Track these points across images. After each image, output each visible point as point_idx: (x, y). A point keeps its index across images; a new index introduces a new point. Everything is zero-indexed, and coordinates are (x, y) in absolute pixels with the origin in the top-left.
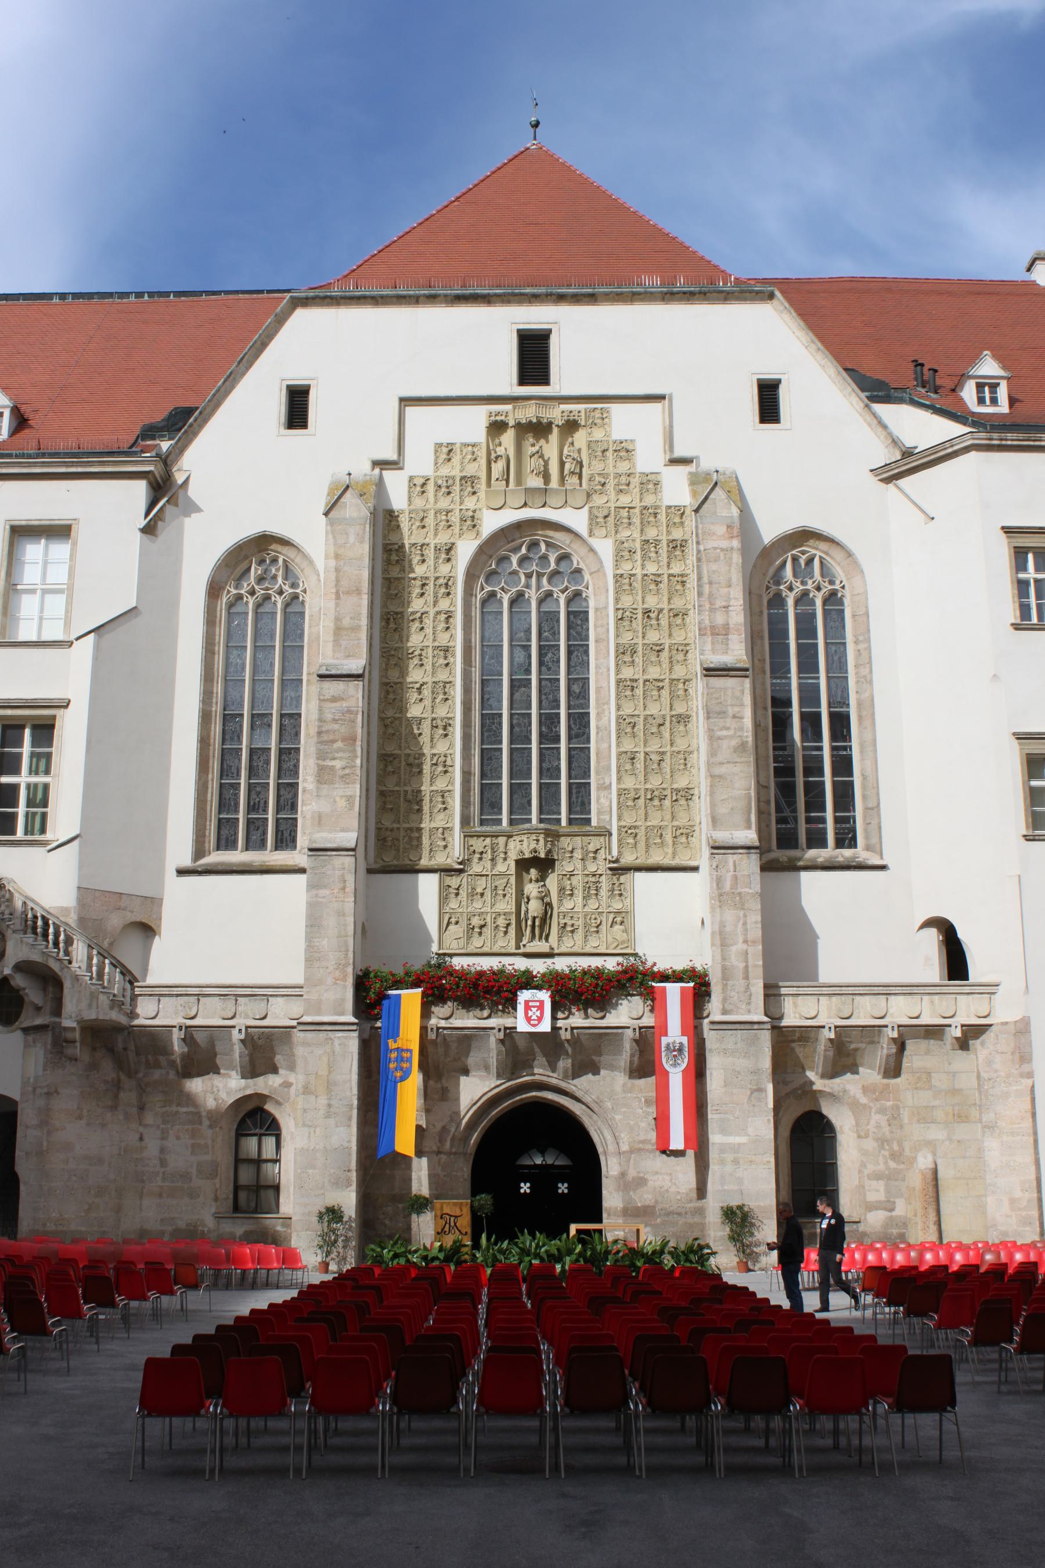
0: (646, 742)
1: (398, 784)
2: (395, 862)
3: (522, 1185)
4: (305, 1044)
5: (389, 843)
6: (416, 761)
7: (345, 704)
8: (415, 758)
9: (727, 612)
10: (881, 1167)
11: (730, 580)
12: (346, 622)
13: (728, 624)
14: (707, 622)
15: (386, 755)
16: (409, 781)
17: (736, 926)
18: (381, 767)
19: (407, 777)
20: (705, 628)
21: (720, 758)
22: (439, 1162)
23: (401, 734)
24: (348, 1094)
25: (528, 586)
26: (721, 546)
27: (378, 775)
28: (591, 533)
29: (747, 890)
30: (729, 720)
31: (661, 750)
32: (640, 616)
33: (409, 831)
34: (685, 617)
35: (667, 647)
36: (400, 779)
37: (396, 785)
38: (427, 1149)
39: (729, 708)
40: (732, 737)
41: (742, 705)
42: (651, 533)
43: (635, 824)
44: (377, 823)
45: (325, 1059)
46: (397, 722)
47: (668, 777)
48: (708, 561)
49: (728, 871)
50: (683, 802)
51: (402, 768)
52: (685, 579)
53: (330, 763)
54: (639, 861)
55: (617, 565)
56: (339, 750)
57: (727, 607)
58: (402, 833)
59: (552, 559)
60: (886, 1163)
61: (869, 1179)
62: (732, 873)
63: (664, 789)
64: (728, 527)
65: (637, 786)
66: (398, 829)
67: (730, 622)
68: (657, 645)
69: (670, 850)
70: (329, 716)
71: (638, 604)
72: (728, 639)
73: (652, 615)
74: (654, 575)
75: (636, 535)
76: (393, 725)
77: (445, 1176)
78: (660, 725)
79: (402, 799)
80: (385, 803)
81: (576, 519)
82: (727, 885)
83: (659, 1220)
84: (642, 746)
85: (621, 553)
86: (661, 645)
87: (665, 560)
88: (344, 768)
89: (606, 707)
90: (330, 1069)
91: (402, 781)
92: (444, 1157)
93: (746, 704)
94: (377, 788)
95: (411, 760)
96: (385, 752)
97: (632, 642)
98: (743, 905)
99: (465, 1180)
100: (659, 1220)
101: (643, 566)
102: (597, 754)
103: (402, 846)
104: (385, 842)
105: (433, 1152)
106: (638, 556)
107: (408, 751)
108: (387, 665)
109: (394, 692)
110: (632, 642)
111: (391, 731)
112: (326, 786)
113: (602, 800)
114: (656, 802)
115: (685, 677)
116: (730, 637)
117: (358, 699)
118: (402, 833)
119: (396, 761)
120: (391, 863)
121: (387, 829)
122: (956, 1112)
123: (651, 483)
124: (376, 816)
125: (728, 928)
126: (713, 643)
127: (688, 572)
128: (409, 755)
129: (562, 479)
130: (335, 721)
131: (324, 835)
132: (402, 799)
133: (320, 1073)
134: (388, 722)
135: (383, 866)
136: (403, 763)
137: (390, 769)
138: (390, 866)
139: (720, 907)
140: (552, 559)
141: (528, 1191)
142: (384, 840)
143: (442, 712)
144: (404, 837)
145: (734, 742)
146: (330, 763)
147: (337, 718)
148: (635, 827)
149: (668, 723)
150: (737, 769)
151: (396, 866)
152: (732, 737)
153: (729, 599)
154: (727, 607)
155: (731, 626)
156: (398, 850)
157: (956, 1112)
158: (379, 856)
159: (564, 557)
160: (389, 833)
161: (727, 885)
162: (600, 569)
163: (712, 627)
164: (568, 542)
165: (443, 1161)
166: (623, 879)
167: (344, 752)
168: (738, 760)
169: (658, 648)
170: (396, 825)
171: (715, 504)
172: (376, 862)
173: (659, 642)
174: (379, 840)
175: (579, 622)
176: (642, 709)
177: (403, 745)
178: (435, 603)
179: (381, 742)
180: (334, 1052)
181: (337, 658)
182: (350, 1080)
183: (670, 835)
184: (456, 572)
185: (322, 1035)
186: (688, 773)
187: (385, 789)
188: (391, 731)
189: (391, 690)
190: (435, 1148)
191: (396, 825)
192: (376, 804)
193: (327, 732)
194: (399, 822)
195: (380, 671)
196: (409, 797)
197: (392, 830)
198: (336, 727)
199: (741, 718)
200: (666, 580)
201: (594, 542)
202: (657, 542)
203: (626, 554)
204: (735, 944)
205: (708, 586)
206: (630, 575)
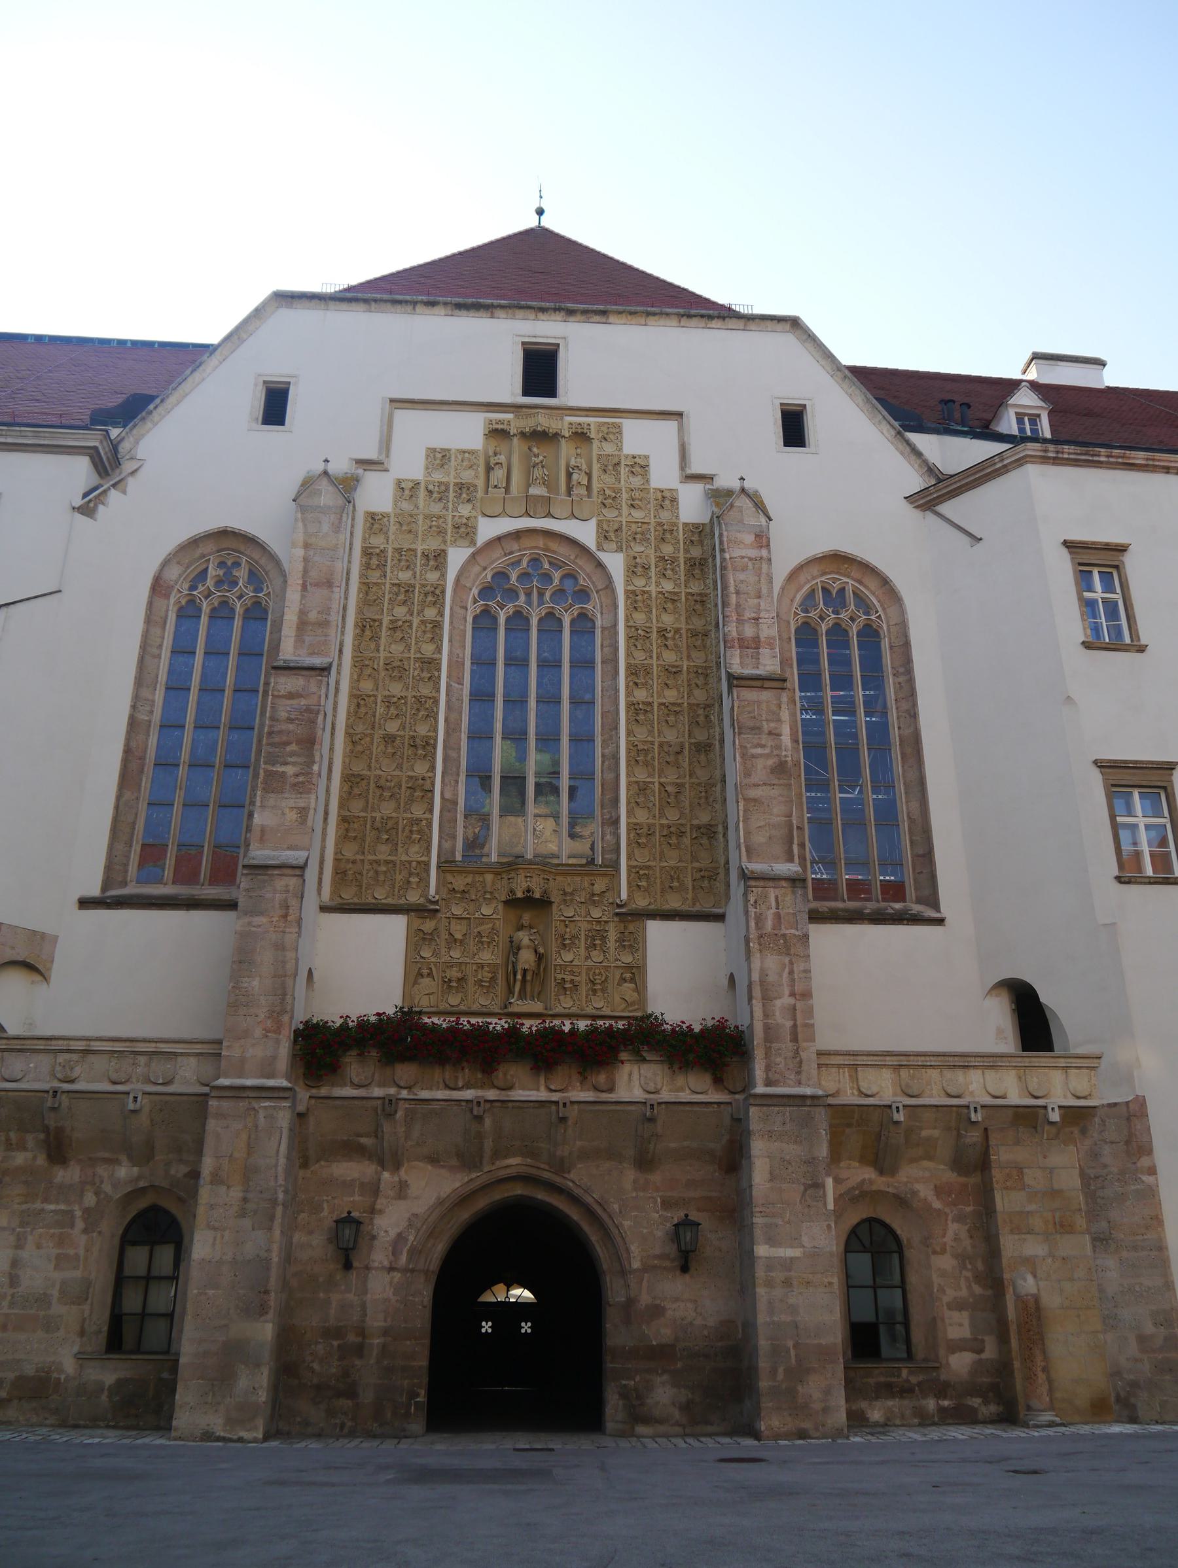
0: (661, 771)
1: (365, 809)
2: (356, 900)
3: (484, 1324)
4: (220, 1116)
5: (350, 877)
6: (388, 784)
7: (303, 702)
8: (387, 781)
9: (757, 625)
10: (964, 1293)
11: (759, 591)
12: (313, 616)
13: (758, 637)
14: (734, 634)
15: (353, 775)
16: (379, 806)
17: (781, 976)
18: (346, 788)
19: (376, 801)
20: (733, 641)
21: (755, 779)
22: (391, 1283)
23: (371, 753)
24: (272, 1183)
25: (529, 602)
26: (749, 555)
27: (341, 797)
28: (600, 548)
29: (793, 931)
30: (764, 736)
31: (678, 781)
32: (654, 635)
33: (375, 865)
34: (705, 638)
35: (685, 668)
36: (367, 803)
37: (362, 811)
38: (376, 1264)
39: (764, 723)
40: (767, 756)
41: (779, 720)
42: (667, 549)
43: (648, 864)
44: (336, 854)
45: (244, 1136)
46: (368, 739)
47: (687, 811)
48: (735, 569)
49: (770, 908)
50: (705, 841)
51: (371, 791)
52: (705, 599)
53: (281, 769)
54: (652, 907)
55: (628, 582)
56: (292, 754)
57: (757, 619)
58: (367, 866)
59: (557, 576)
60: (969, 1287)
61: (950, 1309)
62: (774, 910)
63: (682, 825)
64: (757, 536)
65: (650, 821)
66: (363, 861)
67: (761, 636)
68: (673, 666)
69: (690, 896)
70: (283, 715)
71: (652, 623)
72: (758, 654)
73: (669, 635)
74: (670, 592)
75: (651, 552)
76: (363, 742)
77: (397, 1301)
78: (678, 753)
79: (368, 826)
80: (347, 830)
81: (585, 532)
82: (769, 925)
83: (679, 1365)
84: (657, 776)
85: (634, 569)
86: (677, 667)
87: (683, 578)
88: (297, 776)
89: (613, 733)
90: (250, 1149)
91: (370, 806)
92: (397, 1276)
93: (783, 719)
94: (339, 812)
95: (382, 782)
96: (351, 772)
97: (645, 662)
98: (788, 949)
99: (424, 1307)
100: (679, 1365)
101: (658, 584)
102: (602, 785)
103: (365, 881)
104: (345, 875)
105: (383, 1268)
106: (653, 572)
107: (379, 772)
108: (359, 675)
109: (366, 705)
110: (645, 662)
111: (359, 748)
112: (272, 795)
113: (608, 837)
114: (674, 840)
115: (705, 702)
116: (760, 650)
117: (320, 697)
118: (367, 866)
119: (364, 783)
120: (351, 901)
121: (348, 861)
122: (1057, 1220)
123: (668, 500)
124: (336, 844)
125: (771, 978)
126: (741, 657)
127: (708, 591)
128: (380, 777)
129: (569, 490)
130: (290, 720)
131: (266, 852)
132: (368, 826)
133: (236, 1155)
134: (356, 738)
135: (340, 904)
136: (372, 785)
137: (356, 791)
138: (348, 904)
139: (761, 951)
140: (557, 576)
141: (523, 1324)
142: (345, 873)
143: (422, 730)
144: (368, 871)
145: (770, 762)
146: (281, 769)
147: (293, 717)
148: (648, 867)
149: (686, 751)
150: (775, 792)
151: (355, 904)
152: (767, 756)
153: (759, 611)
154: (757, 619)
155: (763, 639)
156: (361, 886)
157: (1057, 1220)
158: (335, 891)
159: (571, 576)
160: (350, 865)
161: (769, 925)
162: (610, 586)
163: (741, 640)
164: (572, 557)
165: (396, 1280)
166: (631, 927)
167: (299, 755)
168: (776, 781)
169: (674, 670)
170: (359, 857)
171: (742, 512)
172: (332, 899)
173: (676, 663)
174: (337, 873)
175: (584, 644)
176: (656, 735)
177: (373, 765)
178: (421, 612)
179: (347, 761)
180: (257, 1127)
181: (299, 655)
182: (276, 1166)
183: (690, 879)
184: (445, 581)
185: (243, 1104)
186: (710, 808)
187: (349, 814)
188: (359, 748)
189: (362, 702)
190: (386, 1263)
191: (359, 857)
192: (337, 831)
193: (280, 732)
194: (363, 853)
195: (351, 682)
196: (378, 824)
197: (354, 862)
198: (291, 727)
199: (780, 735)
200: (683, 599)
201: (604, 557)
202: (674, 560)
203: (639, 570)
204: (780, 998)
205: (734, 595)
206: (644, 592)
